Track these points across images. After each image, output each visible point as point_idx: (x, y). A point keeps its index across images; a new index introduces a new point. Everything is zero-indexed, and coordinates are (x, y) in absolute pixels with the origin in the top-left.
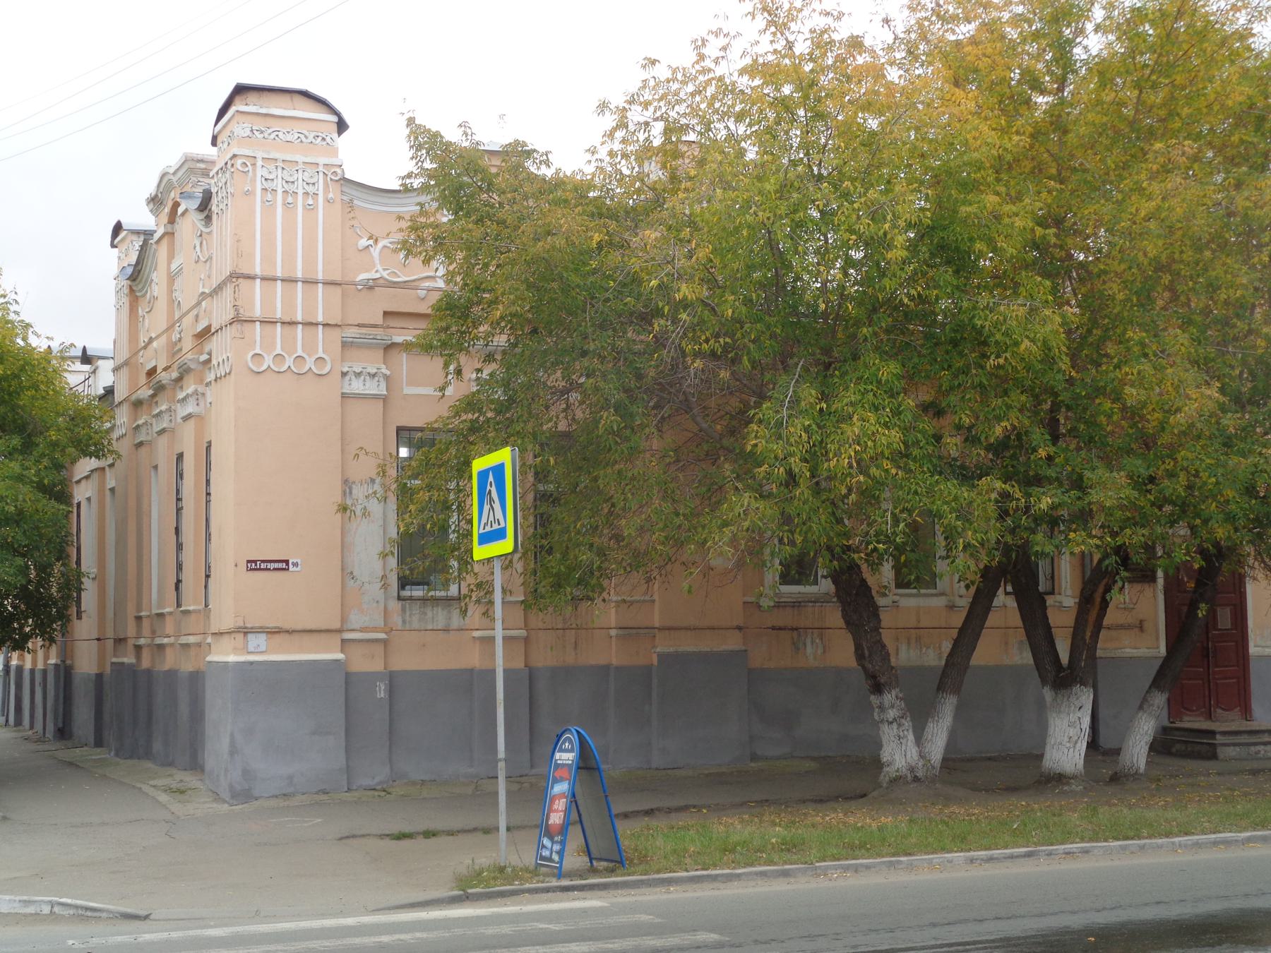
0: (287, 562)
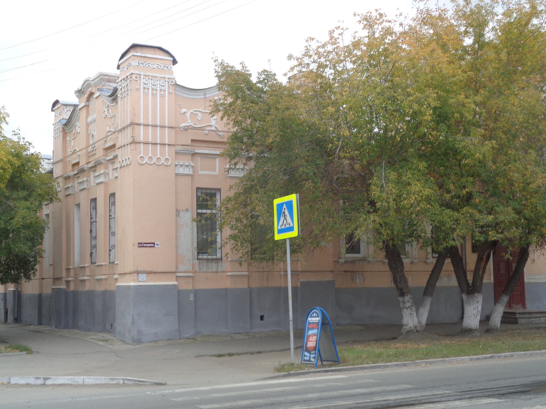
0: (154, 244)
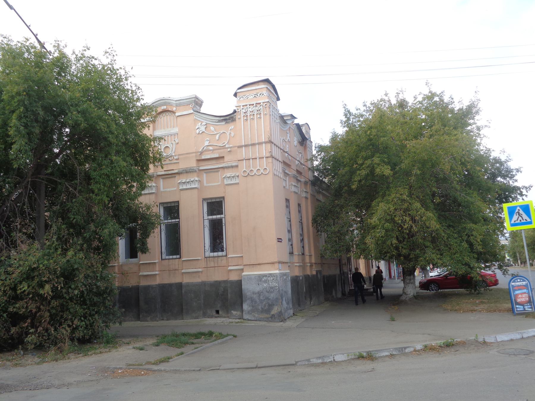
0: (281, 239)
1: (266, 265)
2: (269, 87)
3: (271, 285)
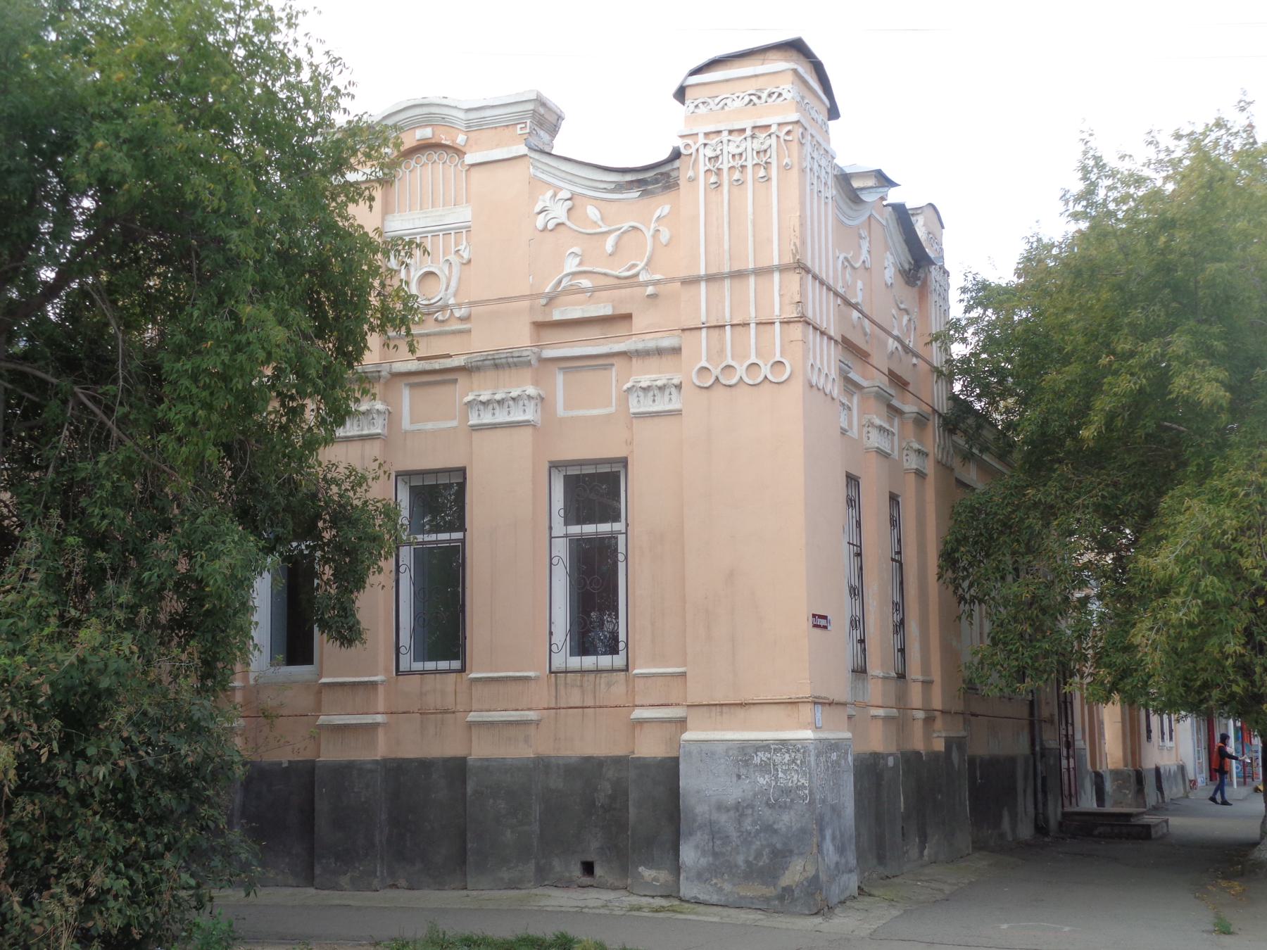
0: (825, 617)
1: (767, 708)
2: (801, 70)
3: (782, 783)
